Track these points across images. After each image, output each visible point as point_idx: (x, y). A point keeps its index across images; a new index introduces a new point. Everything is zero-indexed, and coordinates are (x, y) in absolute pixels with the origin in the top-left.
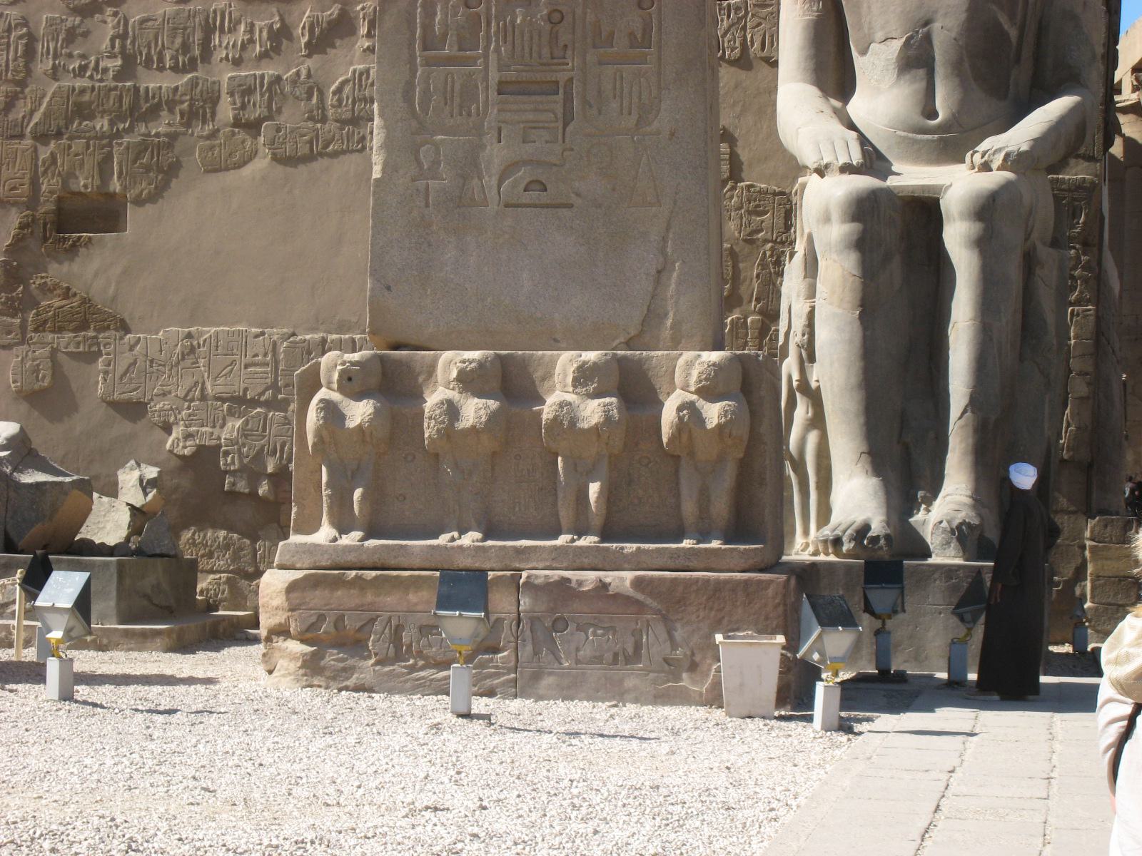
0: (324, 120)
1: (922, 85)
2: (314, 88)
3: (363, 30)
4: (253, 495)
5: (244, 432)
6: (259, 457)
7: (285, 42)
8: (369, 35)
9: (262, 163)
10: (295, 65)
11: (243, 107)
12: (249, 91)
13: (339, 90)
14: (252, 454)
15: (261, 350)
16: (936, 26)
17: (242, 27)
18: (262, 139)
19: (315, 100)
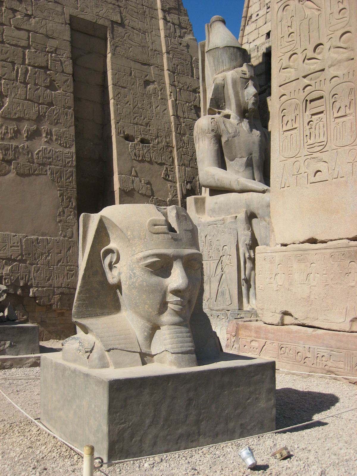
0: (33, 163)
1: (252, 171)
2: (29, 152)
3: (44, 135)
4: (15, 294)
5: (12, 271)
6: (17, 280)
7: (19, 135)
8: (46, 137)
9: (12, 175)
10: (22, 143)
11: (6, 155)
12: (7, 149)
13: (38, 154)
14: (15, 279)
15: (16, 242)
16: (253, 155)
17: (4, 127)
18: (12, 167)
19: (30, 156)
